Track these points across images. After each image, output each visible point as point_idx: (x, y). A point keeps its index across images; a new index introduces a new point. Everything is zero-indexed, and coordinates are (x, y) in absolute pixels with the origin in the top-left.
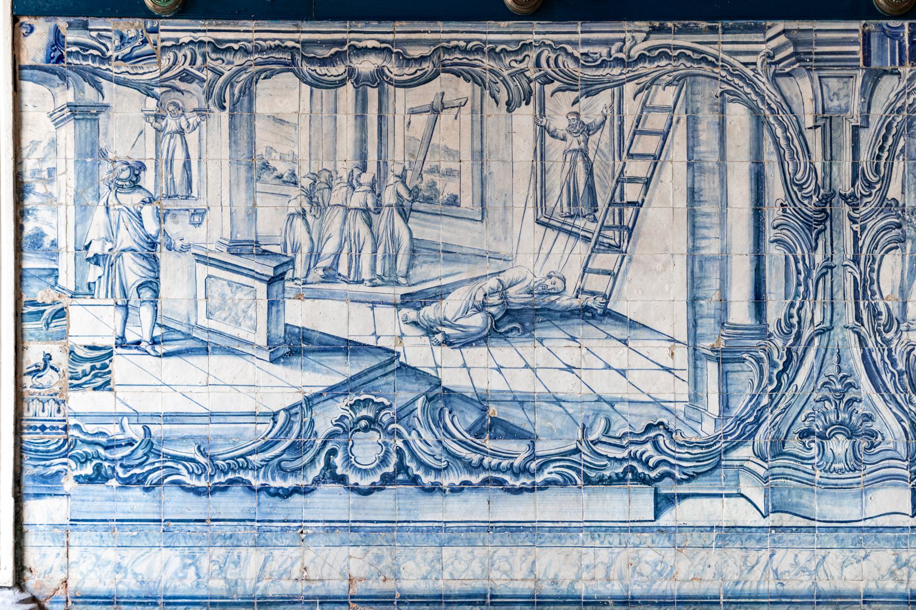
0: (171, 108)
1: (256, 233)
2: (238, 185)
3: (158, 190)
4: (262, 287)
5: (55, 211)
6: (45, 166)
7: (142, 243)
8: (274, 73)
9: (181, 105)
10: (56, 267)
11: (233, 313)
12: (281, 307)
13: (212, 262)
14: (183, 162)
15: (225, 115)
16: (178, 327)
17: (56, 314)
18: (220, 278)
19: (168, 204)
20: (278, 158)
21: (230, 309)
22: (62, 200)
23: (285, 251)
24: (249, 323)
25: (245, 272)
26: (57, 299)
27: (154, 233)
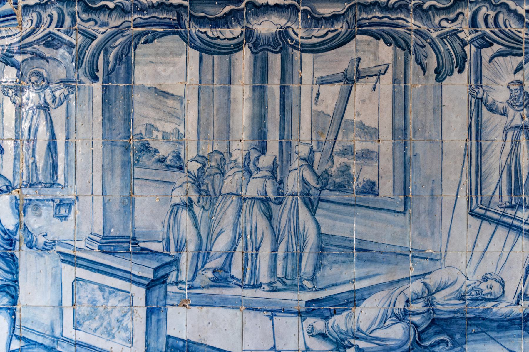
0: (34, 79)
1: (133, 228)
2: (112, 170)
3: (18, 178)
4: (139, 293)
8: (156, 36)
9: (45, 75)
11: (105, 324)
12: (162, 316)
13: (80, 262)
14: (47, 143)
15: (98, 86)
16: (40, 340)
18: (90, 282)
19: (30, 193)
20: (160, 137)
21: (102, 318)
23: (168, 249)
24: (124, 335)
25: (120, 274)
27: (12, 228)
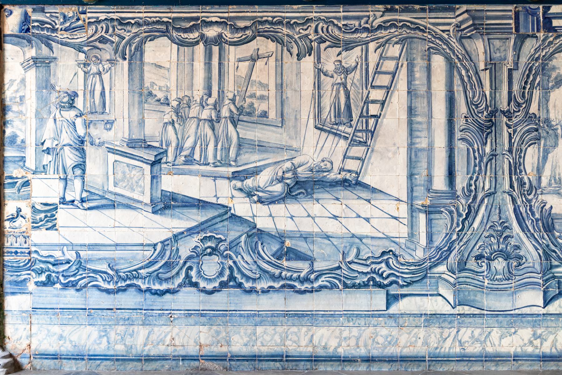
5: (24, 122)
6: (18, 95)
7: (75, 141)
10: (24, 155)
13: (117, 152)
16: (97, 192)
17: (24, 184)
18: (122, 162)
22: (28, 115)
26: (24, 174)
27: (82, 135)
